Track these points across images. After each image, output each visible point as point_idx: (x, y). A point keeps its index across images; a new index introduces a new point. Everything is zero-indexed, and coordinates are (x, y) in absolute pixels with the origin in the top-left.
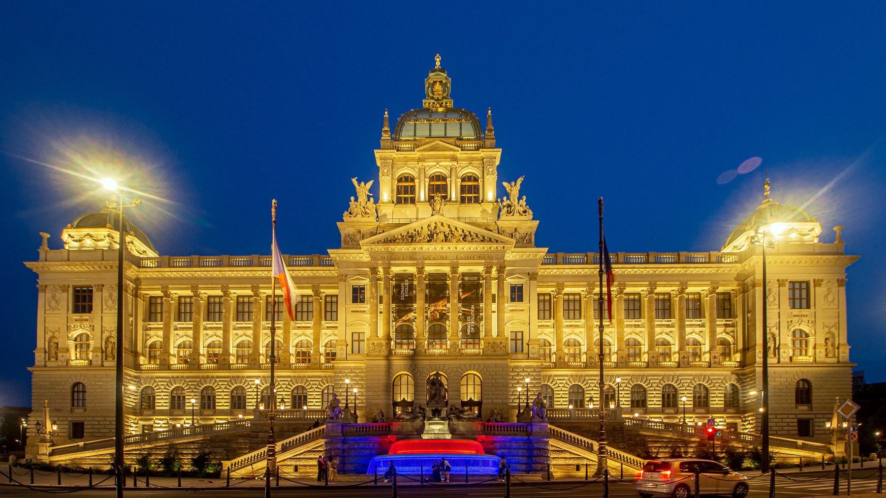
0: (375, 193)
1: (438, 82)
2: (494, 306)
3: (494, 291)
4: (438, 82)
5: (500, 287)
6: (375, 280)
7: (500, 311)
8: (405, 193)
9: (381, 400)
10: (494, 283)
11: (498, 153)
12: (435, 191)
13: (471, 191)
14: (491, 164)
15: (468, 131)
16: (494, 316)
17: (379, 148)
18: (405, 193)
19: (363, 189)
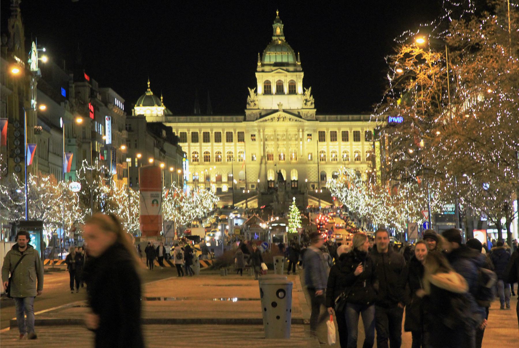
0: (256, 91)
1: (278, 29)
2: (301, 142)
3: (301, 137)
4: (278, 29)
5: (303, 135)
6: (259, 134)
7: (303, 145)
8: (267, 91)
9: (264, 180)
10: (301, 133)
11: (302, 74)
12: (279, 86)
13: (293, 91)
14: (300, 78)
15: (291, 60)
16: (301, 147)
17: (257, 71)
18: (267, 91)
19: (252, 92)
